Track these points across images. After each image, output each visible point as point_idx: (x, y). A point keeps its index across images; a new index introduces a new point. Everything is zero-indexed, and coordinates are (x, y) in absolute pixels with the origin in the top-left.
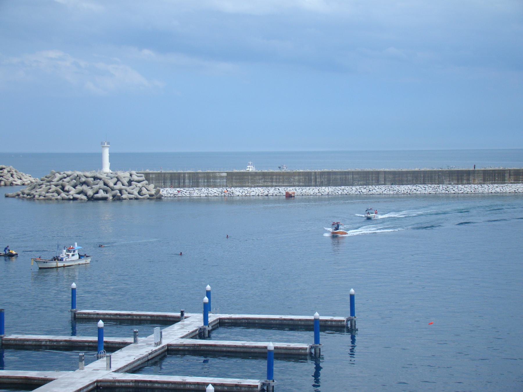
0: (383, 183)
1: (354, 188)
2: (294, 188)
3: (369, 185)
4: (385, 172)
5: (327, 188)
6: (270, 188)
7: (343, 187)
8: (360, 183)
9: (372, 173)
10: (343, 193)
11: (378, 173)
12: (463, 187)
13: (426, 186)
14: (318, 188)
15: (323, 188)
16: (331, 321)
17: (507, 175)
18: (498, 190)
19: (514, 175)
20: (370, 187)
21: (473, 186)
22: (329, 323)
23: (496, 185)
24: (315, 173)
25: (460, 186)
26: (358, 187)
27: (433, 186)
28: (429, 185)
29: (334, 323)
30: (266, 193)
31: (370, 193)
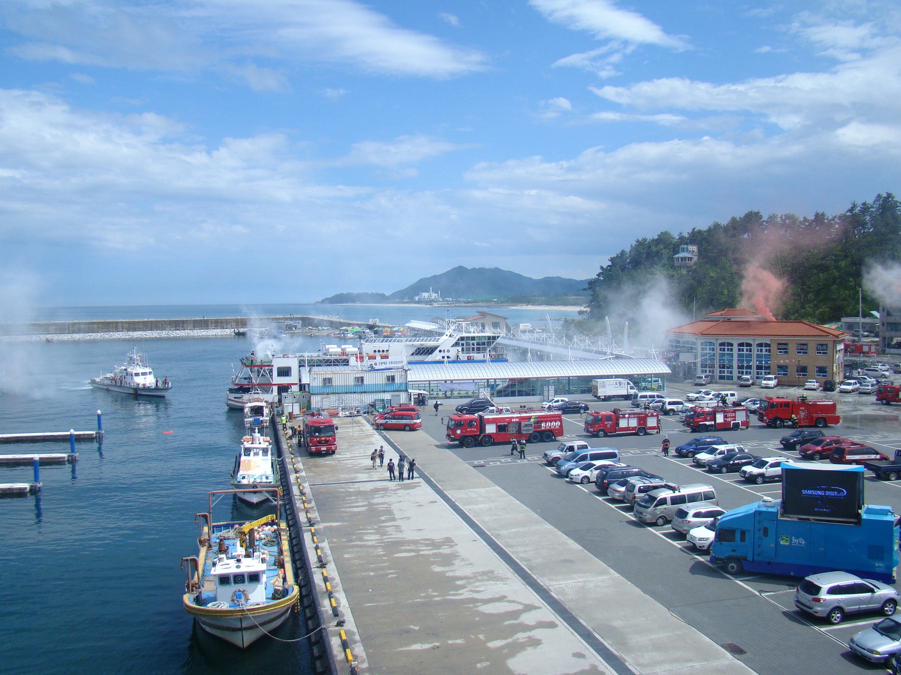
0: (121, 330)
1: (99, 334)
2: (52, 335)
3: (110, 332)
4: (122, 322)
5: (78, 335)
6: (32, 336)
7: (90, 334)
8: (103, 330)
9: (112, 323)
10: (91, 338)
11: (117, 323)
12: (179, 332)
13: (153, 332)
14: (71, 335)
15: (75, 335)
16: (84, 435)
17: (210, 323)
18: (204, 334)
19: (215, 323)
20: (112, 333)
21: (186, 331)
22: (82, 436)
23: (202, 330)
24: (69, 323)
25: (177, 331)
26: (102, 334)
27: (158, 332)
28: (155, 331)
29: (86, 436)
30: (30, 339)
31: (112, 337)
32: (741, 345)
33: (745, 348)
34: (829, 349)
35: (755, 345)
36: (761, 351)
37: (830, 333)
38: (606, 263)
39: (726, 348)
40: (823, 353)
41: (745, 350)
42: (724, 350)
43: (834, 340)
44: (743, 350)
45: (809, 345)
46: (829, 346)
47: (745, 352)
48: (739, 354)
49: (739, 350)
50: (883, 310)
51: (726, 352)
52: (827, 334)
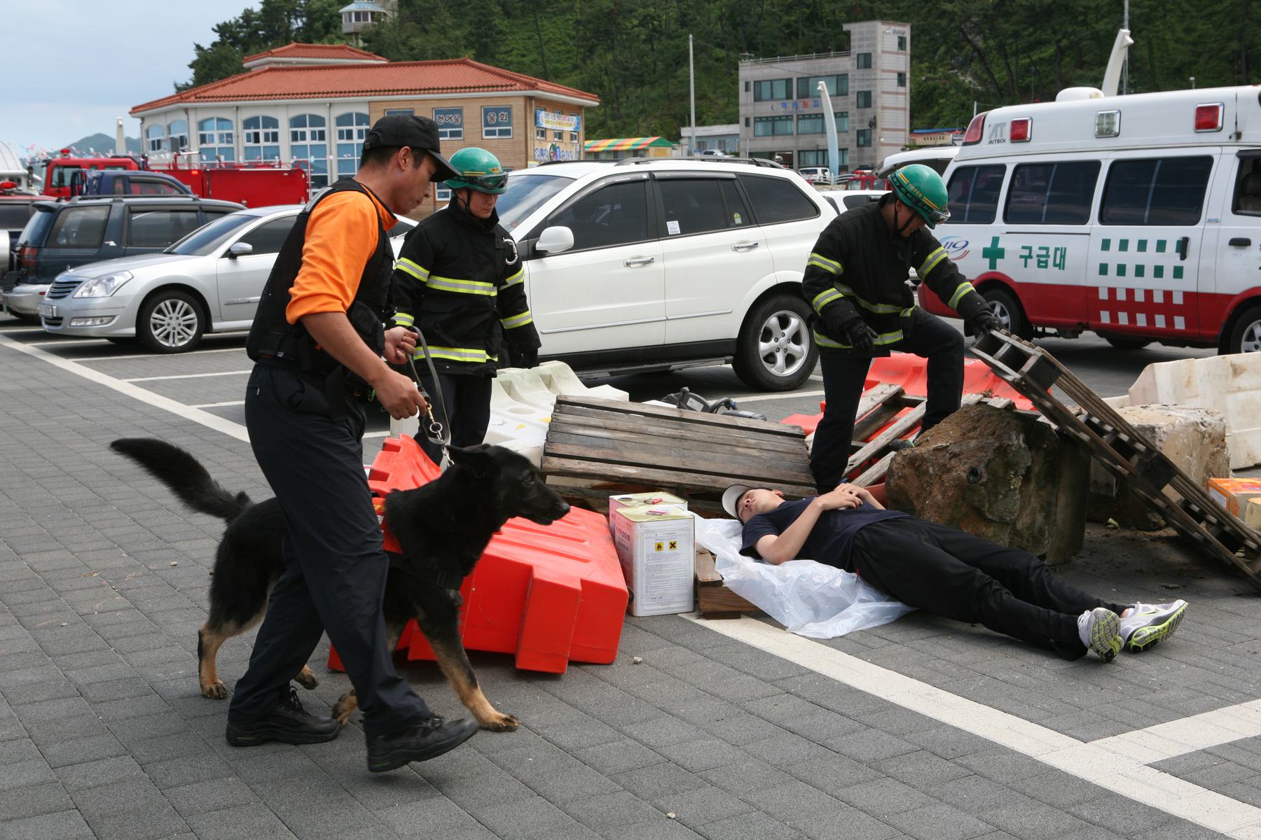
32: (298, 121)
33: (308, 130)
34: (514, 121)
35: (333, 122)
36: (349, 135)
37: (517, 81)
38: (209, 39)
39: (262, 132)
40: (502, 133)
41: (308, 136)
42: (257, 140)
43: (530, 98)
44: (303, 137)
45: (465, 112)
46: (514, 111)
47: (308, 141)
48: (292, 146)
49: (295, 136)
50: (747, 84)
51: (262, 143)
52: (509, 82)
